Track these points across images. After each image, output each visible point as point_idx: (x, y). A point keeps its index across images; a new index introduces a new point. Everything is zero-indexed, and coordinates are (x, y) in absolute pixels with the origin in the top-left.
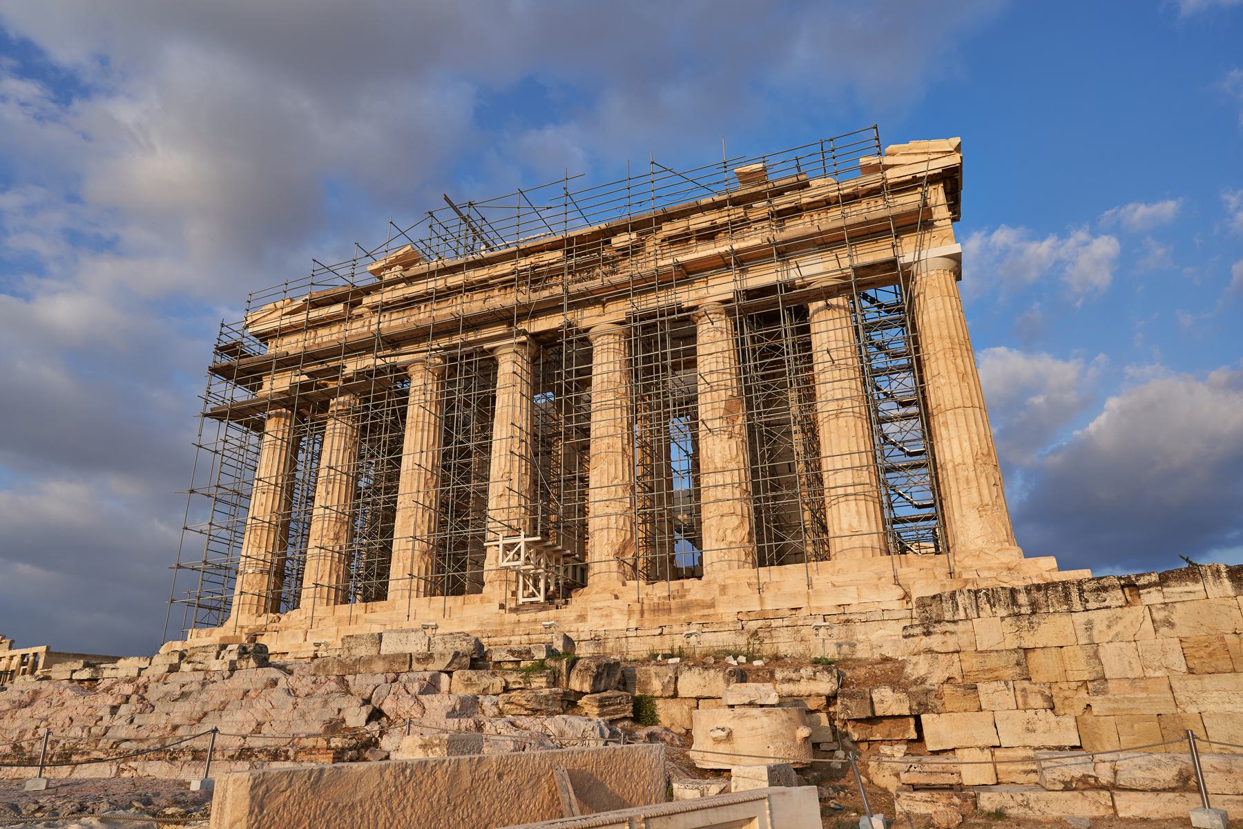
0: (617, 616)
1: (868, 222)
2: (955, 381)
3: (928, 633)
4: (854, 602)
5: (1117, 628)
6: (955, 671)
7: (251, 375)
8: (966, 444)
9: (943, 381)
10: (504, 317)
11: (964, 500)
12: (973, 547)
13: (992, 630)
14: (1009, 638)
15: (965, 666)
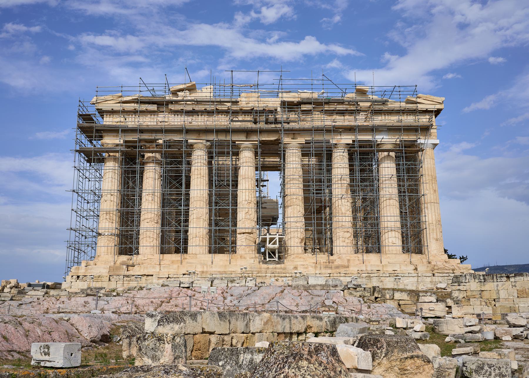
0: (310, 268)
1: (411, 126)
2: (432, 192)
3: (459, 285)
4: (399, 270)
5: (504, 287)
6: (465, 295)
7: (101, 132)
8: (434, 217)
9: (427, 192)
10: (248, 132)
11: (431, 236)
12: (433, 253)
13: (474, 285)
14: (478, 287)
15: (467, 294)
